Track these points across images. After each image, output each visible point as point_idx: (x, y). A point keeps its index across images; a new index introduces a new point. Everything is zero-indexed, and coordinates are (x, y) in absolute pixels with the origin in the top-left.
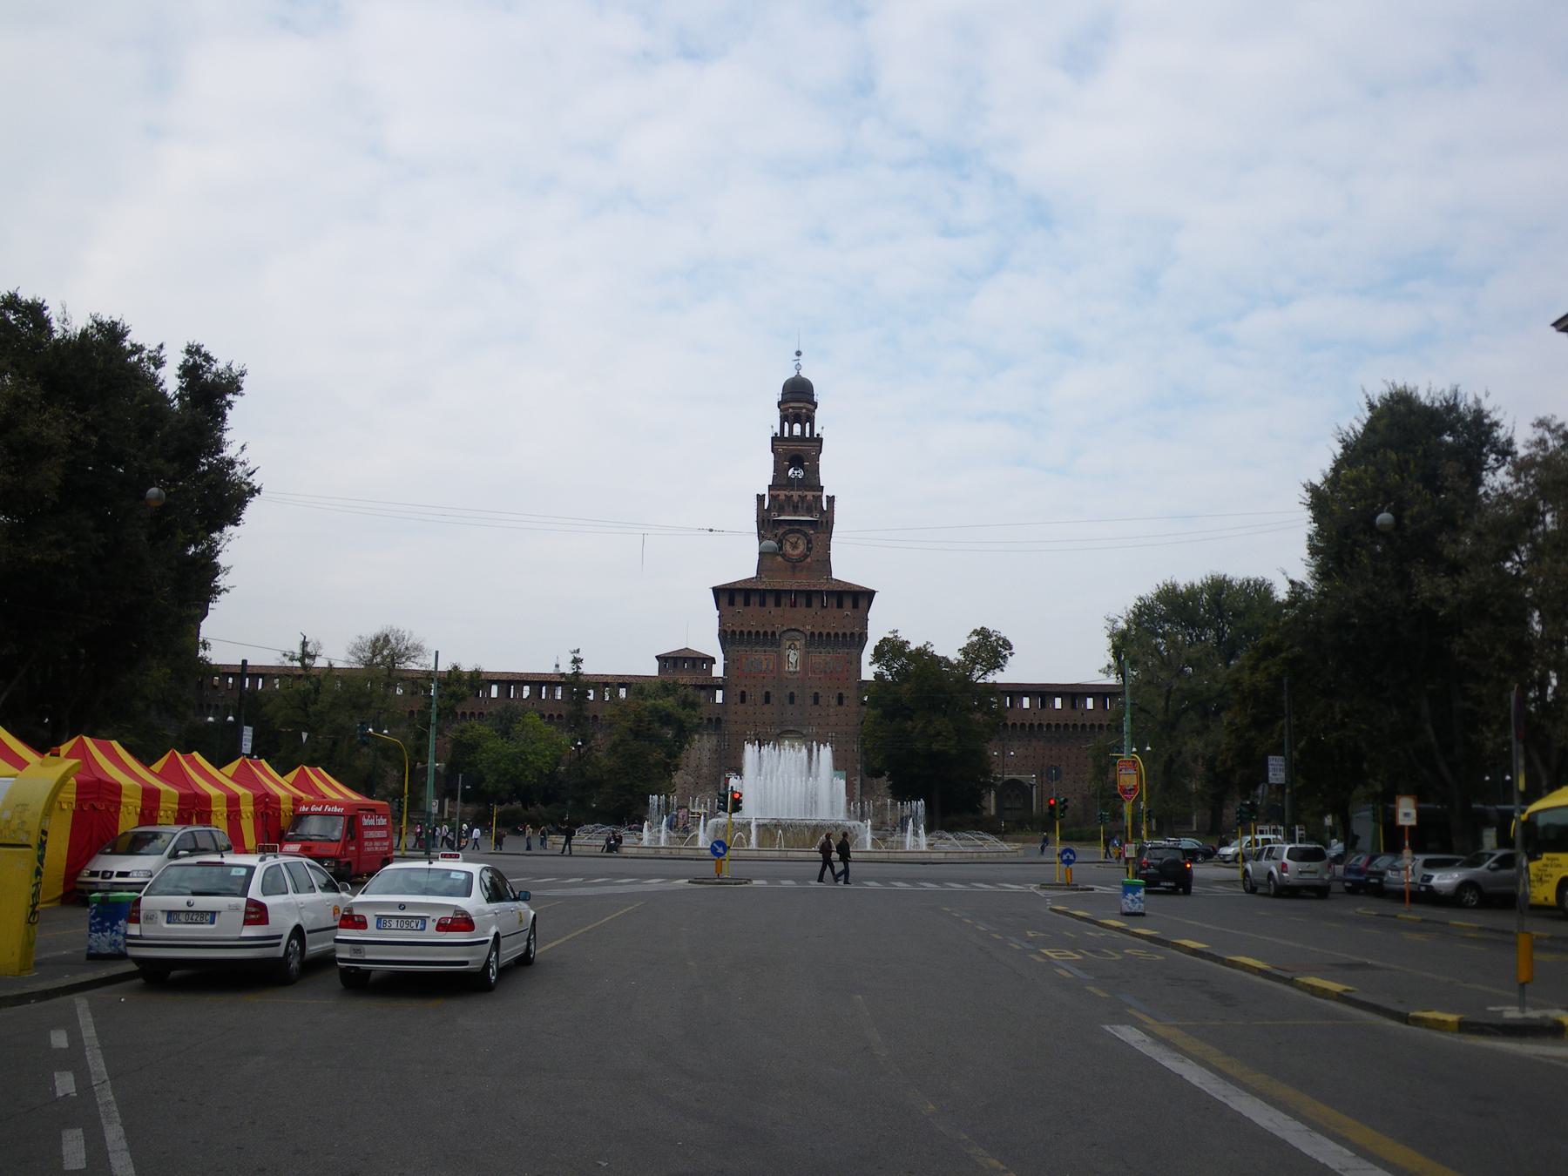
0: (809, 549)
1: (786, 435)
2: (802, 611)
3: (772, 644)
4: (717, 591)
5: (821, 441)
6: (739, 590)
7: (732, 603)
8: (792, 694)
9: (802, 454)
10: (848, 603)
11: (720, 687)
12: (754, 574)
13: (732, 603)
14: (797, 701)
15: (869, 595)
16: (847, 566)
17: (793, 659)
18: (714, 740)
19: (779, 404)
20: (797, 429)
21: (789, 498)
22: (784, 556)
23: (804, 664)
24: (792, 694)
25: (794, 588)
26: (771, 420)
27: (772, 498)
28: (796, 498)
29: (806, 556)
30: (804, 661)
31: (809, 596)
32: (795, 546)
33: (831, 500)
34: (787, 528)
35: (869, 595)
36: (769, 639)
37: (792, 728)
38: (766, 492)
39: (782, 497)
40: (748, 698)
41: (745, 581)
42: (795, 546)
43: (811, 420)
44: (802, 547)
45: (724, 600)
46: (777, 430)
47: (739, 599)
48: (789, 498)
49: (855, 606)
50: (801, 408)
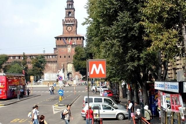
1: (68, 8)
4: (55, 38)
6: (59, 37)
7: (58, 40)
8: (69, 56)
11: (56, 55)
12: (62, 34)
14: (70, 57)
17: (69, 50)
18: (56, 65)
19: (67, 2)
22: (67, 31)
23: (71, 50)
24: (69, 56)
25: (69, 36)
27: (65, 20)
28: (69, 20)
29: (71, 31)
30: (71, 49)
34: (68, 25)
36: (66, 46)
37: (69, 62)
39: (67, 20)
40: (61, 57)
41: (61, 36)
44: (71, 29)
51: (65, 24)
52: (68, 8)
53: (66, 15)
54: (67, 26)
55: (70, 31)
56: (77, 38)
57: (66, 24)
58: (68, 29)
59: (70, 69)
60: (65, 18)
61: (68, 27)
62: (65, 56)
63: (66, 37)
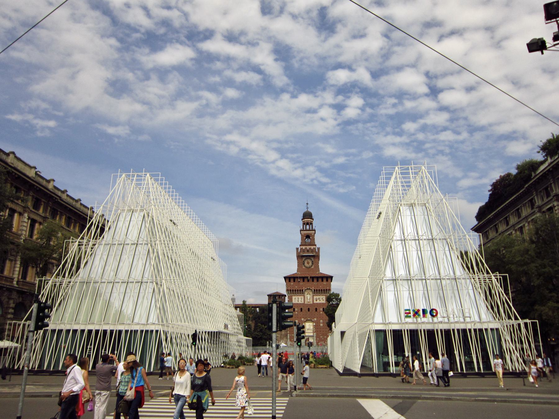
0: (312, 264)
1: (305, 229)
2: (311, 282)
3: (303, 293)
4: (285, 278)
5: (315, 230)
7: (290, 281)
9: (310, 235)
10: (325, 280)
13: (290, 281)
15: (331, 278)
16: (324, 268)
17: (308, 298)
19: (302, 220)
20: (308, 227)
21: (306, 248)
22: (305, 266)
26: (299, 225)
27: (301, 249)
29: (312, 266)
31: (313, 278)
32: (308, 263)
33: (319, 249)
35: (331, 278)
37: (309, 319)
38: (299, 246)
41: (294, 274)
42: (308, 263)
43: (311, 224)
44: (310, 264)
45: (288, 280)
46: (302, 227)
47: (292, 280)
48: (306, 248)
49: (327, 281)
50: (309, 221)
51: (301, 257)
52: (305, 229)
53: (302, 240)
54: (304, 259)
55: (310, 267)
56: (318, 278)
57: (302, 256)
58: (306, 264)
59: (309, 331)
60: (300, 246)
61: (305, 260)
62: (301, 309)
63: (303, 276)
